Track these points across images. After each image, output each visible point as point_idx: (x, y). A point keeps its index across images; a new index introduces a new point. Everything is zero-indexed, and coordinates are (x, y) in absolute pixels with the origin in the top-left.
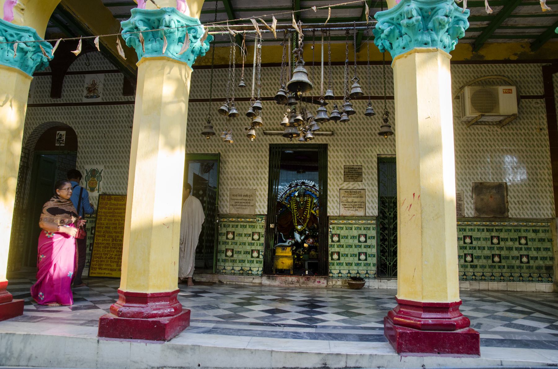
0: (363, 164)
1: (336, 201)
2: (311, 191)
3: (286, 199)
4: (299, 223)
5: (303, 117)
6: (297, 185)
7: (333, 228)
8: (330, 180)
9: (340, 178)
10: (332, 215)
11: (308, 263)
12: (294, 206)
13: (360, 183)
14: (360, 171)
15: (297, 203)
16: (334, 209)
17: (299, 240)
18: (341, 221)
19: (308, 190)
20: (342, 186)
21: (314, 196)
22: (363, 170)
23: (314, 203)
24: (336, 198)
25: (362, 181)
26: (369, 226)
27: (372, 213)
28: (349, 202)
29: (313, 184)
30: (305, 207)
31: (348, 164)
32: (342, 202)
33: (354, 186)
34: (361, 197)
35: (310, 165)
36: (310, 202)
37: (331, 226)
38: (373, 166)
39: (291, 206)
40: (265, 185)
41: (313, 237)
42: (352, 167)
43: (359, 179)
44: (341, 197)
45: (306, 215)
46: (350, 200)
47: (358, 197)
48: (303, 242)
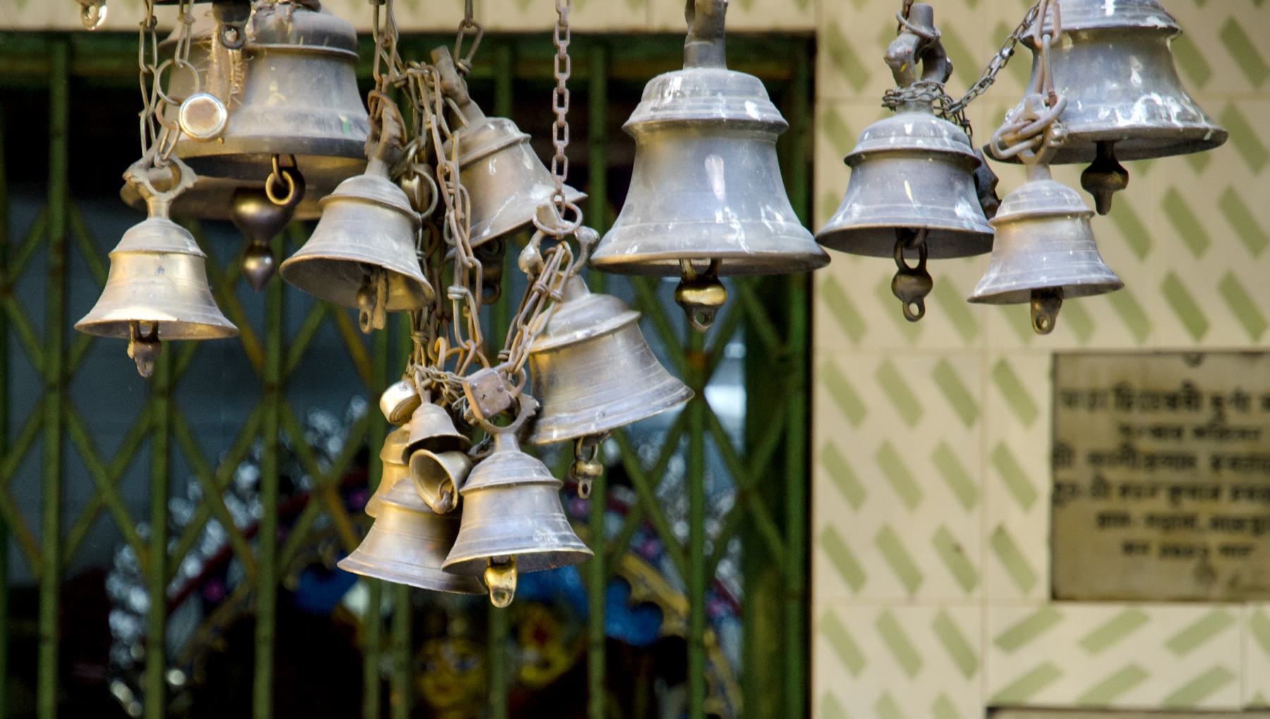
5: (430, 231)
8: (853, 576)
9: (1001, 540)
20: (1028, 658)
42: (1174, 376)
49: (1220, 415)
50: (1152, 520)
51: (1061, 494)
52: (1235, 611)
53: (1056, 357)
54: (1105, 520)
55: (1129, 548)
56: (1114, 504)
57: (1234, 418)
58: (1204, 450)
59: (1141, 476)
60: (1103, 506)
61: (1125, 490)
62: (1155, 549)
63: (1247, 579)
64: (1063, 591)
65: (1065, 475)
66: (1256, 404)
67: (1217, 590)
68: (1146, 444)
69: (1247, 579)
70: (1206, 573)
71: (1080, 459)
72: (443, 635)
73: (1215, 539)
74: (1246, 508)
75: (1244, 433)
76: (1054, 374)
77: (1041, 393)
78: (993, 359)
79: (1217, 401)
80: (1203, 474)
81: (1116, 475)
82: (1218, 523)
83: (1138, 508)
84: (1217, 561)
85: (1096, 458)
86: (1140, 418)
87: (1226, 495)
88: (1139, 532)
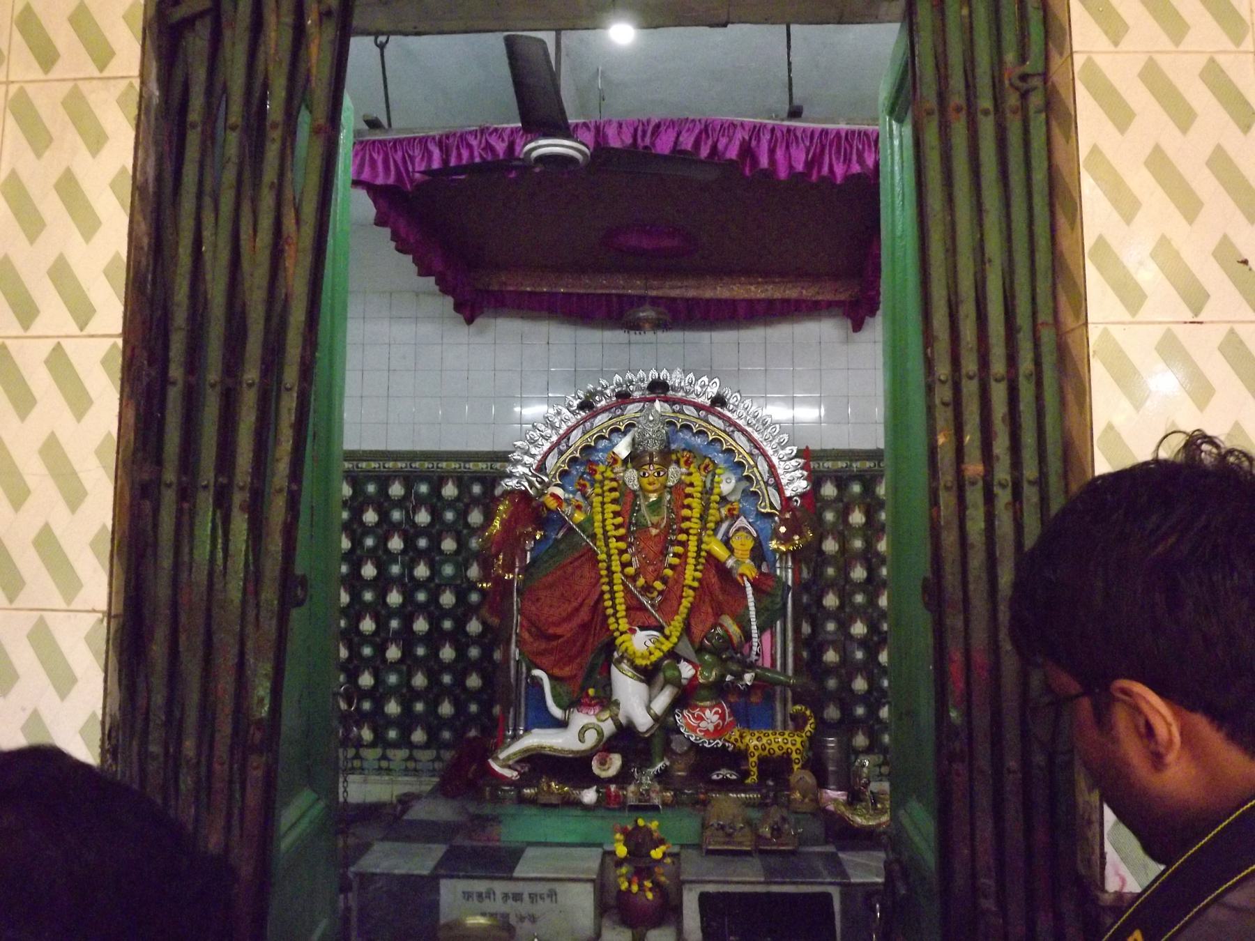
2: (701, 433)
3: (564, 474)
4: (639, 616)
6: (624, 397)
11: (704, 899)
12: (605, 517)
15: (628, 500)
17: (643, 722)
19: (687, 427)
21: (719, 458)
23: (724, 500)
29: (713, 391)
30: (675, 526)
35: (691, 293)
36: (696, 491)
39: (590, 520)
40: (79, 402)
41: (719, 690)
45: (679, 569)
48: (665, 725)
72: (651, 463)
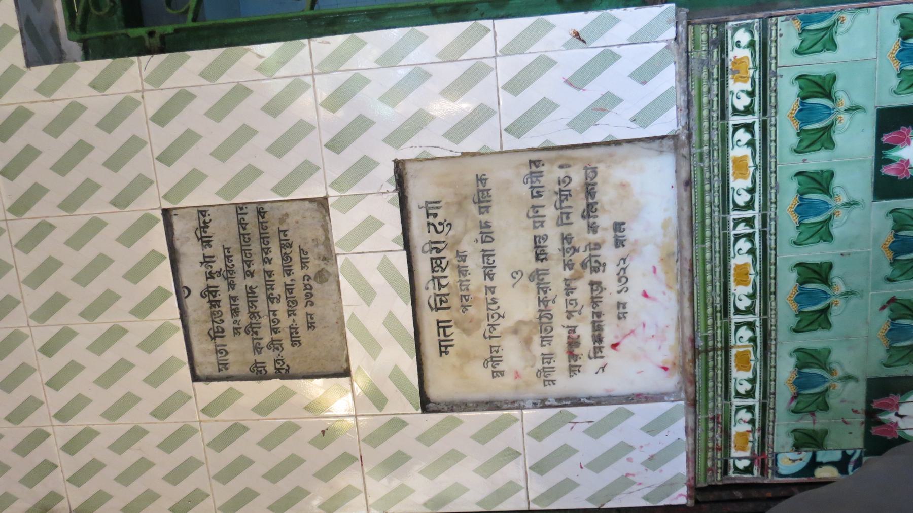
0: (151, 203)
1: (539, 433)
7: (807, 440)
10: (679, 466)
13: (341, 224)
14: (223, 231)
16: (623, 449)
18: (740, 378)
22: (203, 196)
24: (511, 437)
25: (322, 203)
26: (787, 95)
27: (643, 75)
28: (544, 316)
31: (176, 345)
32: (545, 374)
33: (376, 280)
34: (483, 199)
37: (789, 463)
38: (155, 101)
42: (197, 305)
43: (303, 233)
44: (502, 388)
46: (519, 305)
47: (486, 233)
49: (219, 272)
50: (291, 313)
51: (283, 373)
52: (340, 260)
53: (195, 378)
54: (295, 342)
55: (311, 326)
56: (284, 335)
57: (219, 264)
58: (242, 283)
59: (265, 321)
60: (287, 343)
61: (275, 330)
62: (309, 309)
63: (321, 250)
64: (345, 366)
65: (271, 369)
66: (208, 251)
67: (330, 269)
68: (244, 318)
69: (321, 250)
70: (321, 276)
71: (259, 358)
73: (298, 272)
74: (275, 253)
75: (228, 258)
76: (209, 379)
77: (220, 387)
78: (204, 417)
79: (210, 276)
80: (257, 281)
81: (266, 336)
82: (288, 271)
83: (285, 322)
84: (311, 271)
85: (257, 349)
86: (228, 324)
87: (268, 267)
88: (300, 320)
